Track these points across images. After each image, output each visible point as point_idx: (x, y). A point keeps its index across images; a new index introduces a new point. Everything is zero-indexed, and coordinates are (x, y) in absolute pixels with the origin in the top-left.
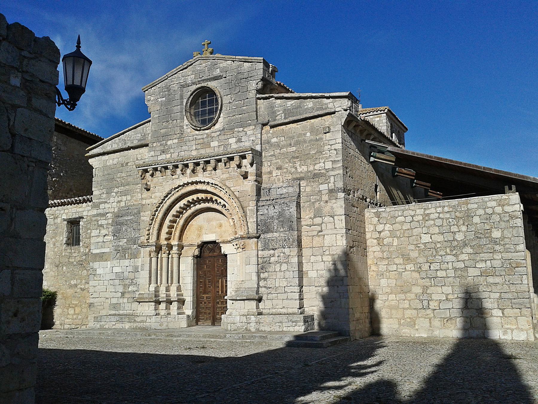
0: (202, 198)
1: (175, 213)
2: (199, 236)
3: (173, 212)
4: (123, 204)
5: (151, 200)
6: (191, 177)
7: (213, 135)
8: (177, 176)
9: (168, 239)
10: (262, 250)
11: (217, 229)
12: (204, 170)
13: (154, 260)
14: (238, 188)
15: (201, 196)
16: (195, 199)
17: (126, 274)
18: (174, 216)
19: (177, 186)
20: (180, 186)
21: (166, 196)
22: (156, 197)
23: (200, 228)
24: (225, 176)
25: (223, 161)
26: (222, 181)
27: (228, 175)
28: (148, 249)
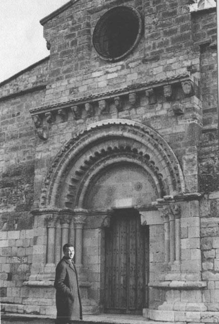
0: (116, 148)
1: (78, 170)
2: (109, 201)
3: (77, 168)
4: (13, 162)
5: (49, 153)
6: (100, 120)
7: (131, 65)
8: (81, 121)
9: (67, 204)
10: (207, 217)
11: (135, 192)
12: (120, 109)
13: (52, 231)
14: (169, 130)
15: (113, 145)
16: (106, 150)
17: (15, 249)
18: (77, 173)
19: (82, 133)
20: (86, 132)
21: (68, 147)
22: (54, 149)
23: (111, 191)
24: (149, 115)
25: (147, 94)
26: (146, 122)
27: (153, 114)
28: (44, 216)
